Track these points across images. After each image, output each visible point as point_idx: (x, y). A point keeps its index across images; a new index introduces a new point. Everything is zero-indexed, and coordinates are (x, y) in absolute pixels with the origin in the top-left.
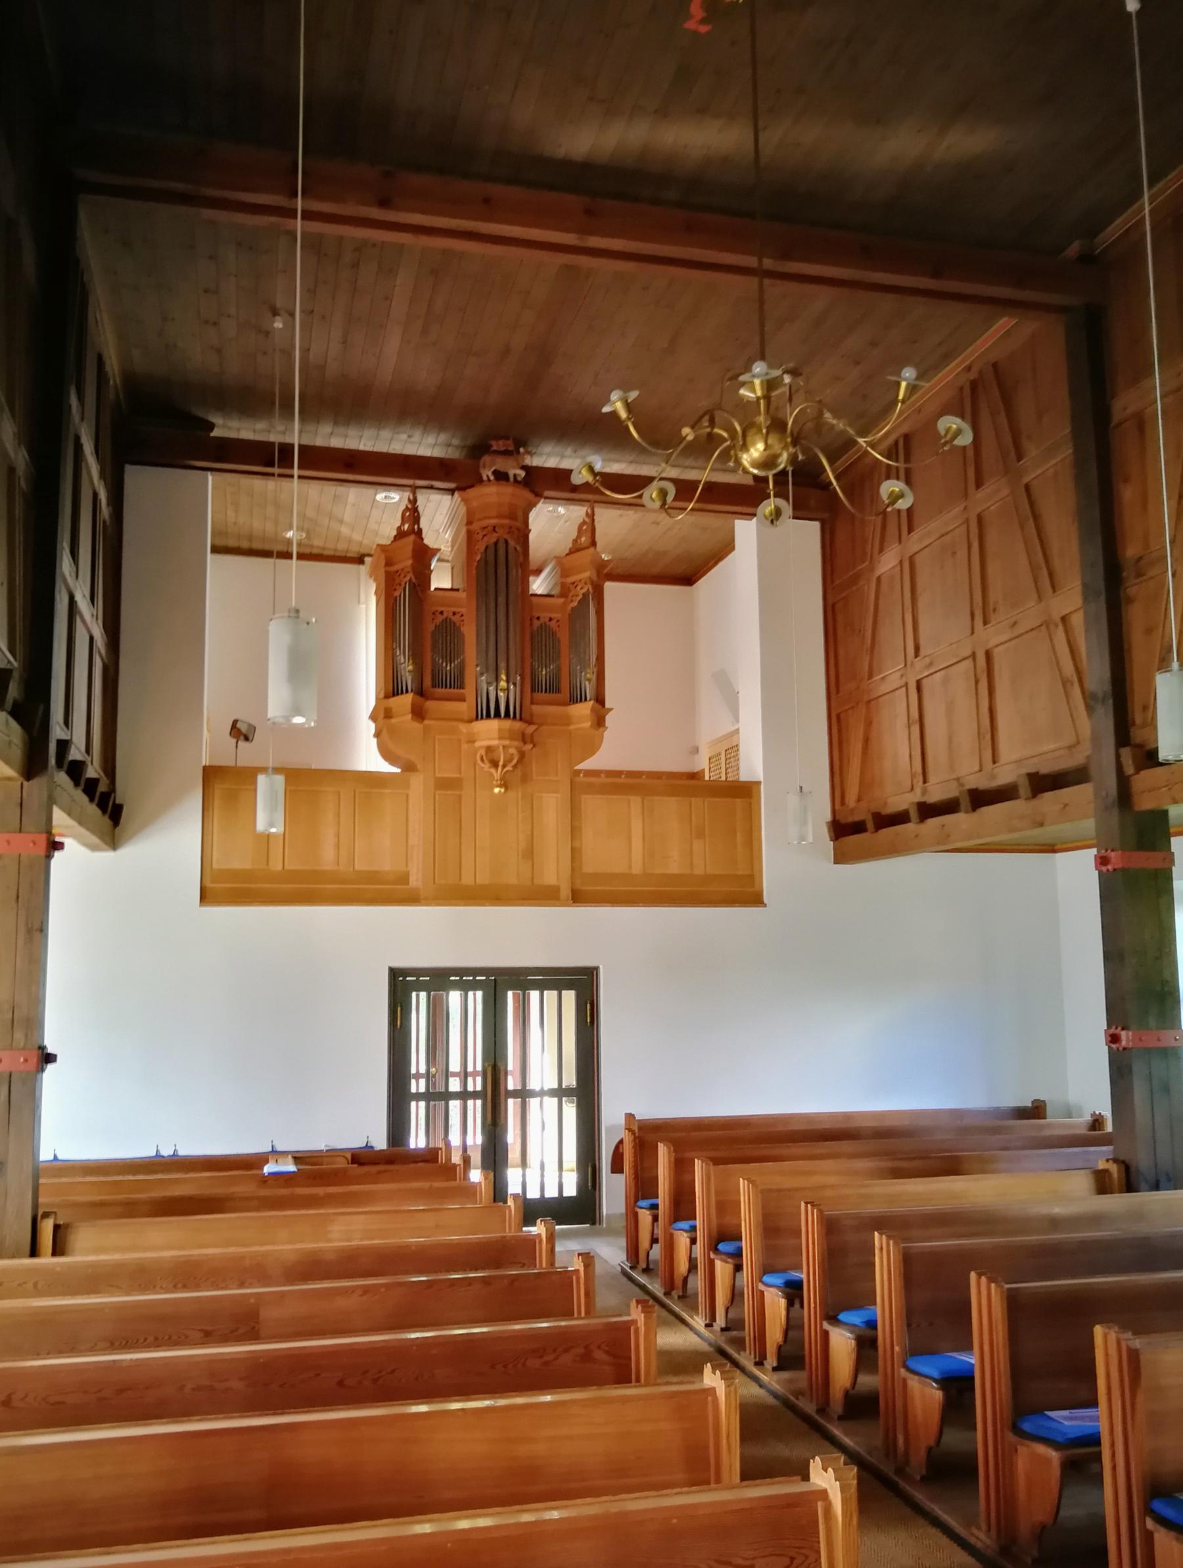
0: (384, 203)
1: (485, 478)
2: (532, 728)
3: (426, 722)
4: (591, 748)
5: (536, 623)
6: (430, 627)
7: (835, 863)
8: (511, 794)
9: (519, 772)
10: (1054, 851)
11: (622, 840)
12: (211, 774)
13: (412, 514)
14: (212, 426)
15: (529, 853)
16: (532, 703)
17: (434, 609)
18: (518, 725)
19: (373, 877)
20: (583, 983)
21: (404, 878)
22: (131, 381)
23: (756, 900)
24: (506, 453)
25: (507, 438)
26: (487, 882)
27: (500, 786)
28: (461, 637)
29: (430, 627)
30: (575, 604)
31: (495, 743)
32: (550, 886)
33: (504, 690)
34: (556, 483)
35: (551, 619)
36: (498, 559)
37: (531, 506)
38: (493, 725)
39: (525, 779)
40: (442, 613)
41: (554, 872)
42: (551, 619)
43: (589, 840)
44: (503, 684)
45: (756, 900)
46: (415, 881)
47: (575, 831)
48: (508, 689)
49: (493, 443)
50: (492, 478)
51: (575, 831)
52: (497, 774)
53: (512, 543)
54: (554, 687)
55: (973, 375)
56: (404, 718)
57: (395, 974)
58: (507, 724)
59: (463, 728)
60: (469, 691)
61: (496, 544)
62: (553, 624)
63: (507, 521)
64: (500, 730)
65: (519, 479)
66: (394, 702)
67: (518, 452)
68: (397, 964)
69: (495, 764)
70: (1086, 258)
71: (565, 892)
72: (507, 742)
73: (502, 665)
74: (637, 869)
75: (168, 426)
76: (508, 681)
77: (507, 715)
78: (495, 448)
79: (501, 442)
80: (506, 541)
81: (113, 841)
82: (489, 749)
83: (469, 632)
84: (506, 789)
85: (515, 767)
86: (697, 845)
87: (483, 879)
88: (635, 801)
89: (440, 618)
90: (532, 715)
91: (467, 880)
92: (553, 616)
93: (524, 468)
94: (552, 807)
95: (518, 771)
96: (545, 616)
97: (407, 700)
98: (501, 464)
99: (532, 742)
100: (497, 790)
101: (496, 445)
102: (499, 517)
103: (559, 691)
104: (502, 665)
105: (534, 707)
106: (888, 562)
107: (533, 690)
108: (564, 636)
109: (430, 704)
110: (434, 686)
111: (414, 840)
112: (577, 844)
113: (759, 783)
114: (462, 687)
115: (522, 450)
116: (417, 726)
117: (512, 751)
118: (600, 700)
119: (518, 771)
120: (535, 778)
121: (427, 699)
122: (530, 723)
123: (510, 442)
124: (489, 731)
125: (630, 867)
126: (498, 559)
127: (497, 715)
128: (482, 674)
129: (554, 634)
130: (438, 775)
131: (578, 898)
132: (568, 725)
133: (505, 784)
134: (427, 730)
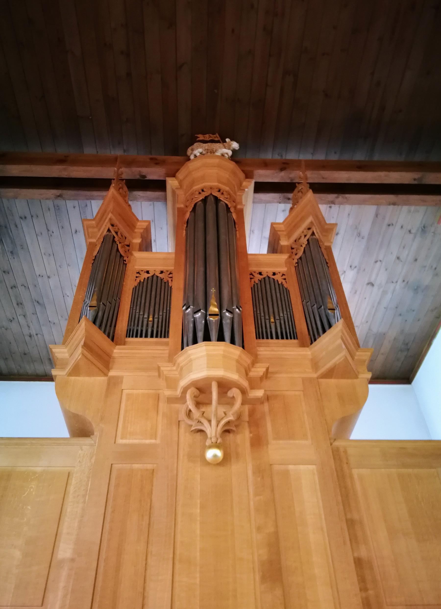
1: (192, 157)
3: (112, 373)
17: (138, 267)
18: (235, 351)
27: (217, 446)
29: (130, 284)
30: (300, 253)
39: (258, 442)
40: (148, 272)
42: (274, 274)
44: (214, 309)
48: (221, 315)
49: (199, 136)
52: (212, 431)
54: (288, 333)
61: (205, 201)
64: (209, 356)
72: (220, 373)
73: (213, 291)
76: (221, 309)
79: (207, 136)
89: (146, 276)
92: (276, 270)
101: (201, 137)
104: (213, 291)
109: (118, 351)
110: (130, 333)
112: (363, 553)
114: (166, 334)
115: (227, 140)
121: (117, 344)
123: (217, 135)
127: (207, 338)
129: (281, 286)
130: (120, 441)
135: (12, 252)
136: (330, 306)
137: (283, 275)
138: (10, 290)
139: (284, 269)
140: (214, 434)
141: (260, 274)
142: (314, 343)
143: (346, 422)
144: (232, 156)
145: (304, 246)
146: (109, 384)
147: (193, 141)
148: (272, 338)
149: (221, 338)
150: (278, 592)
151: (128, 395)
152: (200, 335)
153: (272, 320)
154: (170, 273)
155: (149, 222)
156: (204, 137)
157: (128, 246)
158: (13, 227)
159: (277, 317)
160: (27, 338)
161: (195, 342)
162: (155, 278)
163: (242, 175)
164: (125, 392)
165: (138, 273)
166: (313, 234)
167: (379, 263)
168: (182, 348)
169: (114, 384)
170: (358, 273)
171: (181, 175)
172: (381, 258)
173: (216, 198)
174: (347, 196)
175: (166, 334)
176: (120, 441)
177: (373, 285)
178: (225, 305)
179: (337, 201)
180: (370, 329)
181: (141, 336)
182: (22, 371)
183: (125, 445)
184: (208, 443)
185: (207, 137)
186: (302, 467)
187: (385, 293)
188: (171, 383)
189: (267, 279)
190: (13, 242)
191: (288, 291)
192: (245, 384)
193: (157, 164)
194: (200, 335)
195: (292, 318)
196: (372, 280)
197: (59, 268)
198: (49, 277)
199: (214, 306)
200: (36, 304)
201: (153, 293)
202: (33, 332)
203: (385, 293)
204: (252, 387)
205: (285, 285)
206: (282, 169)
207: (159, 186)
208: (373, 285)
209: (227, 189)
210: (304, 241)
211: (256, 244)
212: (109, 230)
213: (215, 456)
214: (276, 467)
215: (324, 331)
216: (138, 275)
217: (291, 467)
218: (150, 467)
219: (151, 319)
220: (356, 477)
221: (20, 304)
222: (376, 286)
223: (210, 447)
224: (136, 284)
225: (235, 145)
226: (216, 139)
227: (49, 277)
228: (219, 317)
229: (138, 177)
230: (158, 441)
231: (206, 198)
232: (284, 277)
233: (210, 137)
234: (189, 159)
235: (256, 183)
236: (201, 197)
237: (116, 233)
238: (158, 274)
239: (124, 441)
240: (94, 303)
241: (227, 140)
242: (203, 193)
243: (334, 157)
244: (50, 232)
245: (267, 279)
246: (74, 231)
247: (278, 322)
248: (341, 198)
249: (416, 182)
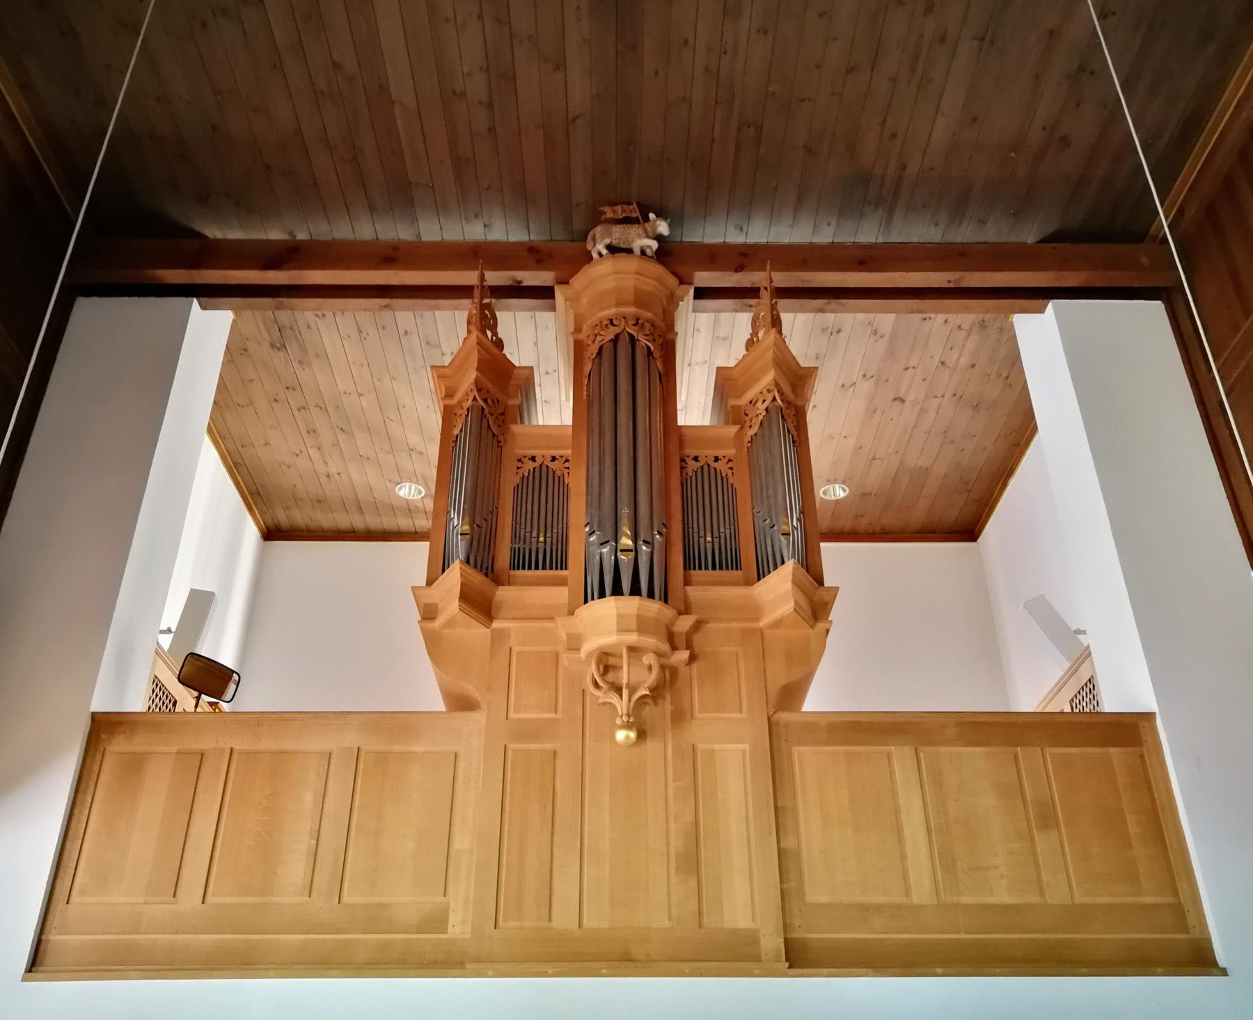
1: (595, 255)
2: (684, 624)
3: (496, 624)
5: (692, 466)
6: (510, 480)
8: (652, 746)
12: (103, 727)
15: (692, 860)
17: (520, 452)
18: (654, 607)
19: (375, 918)
21: (437, 921)
24: (627, 221)
25: (630, 204)
26: (605, 924)
27: (628, 726)
29: (510, 480)
30: (755, 430)
32: (736, 932)
35: (717, 459)
38: (608, 608)
39: (680, 717)
40: (533, 459)
41: (744, 903)
42: (717, 459)
44: (626, 542)
45: (1198, 959)
47: (782, 816)
49: (606, 209)
50: (604, 252)
51: (782, 816)
52: (622, 705)
53: (643, 340)
54: (727, 560)
56: (452, 607)
58: (631, 605)
62: (721, 466)
63: (631, 310)
64: (620, 617)
65: (649, 252)
67: (647, 219)
71: (772, 943)
72: (633, 638)
73: (625, 512)
74: (922, 893)
76: (635, 538)
78: (609, 215)
79: (618, 208)
80: (633, 340)
83: (577, 483)
84: (642, 735)
86: (1044, 842)
89: (531, 465)
91: (565, 919)
92: (720, 453)
93: (659, 238)
96: (707, 453)
98: (618, 234)
99: (689, 646)
100: (621, 735)
102: (619, 304)
103: (737, 566)
104: (625, 512)
105: (688, 588)
107: (687, 567)
108: (740, 481)
109: (504, 594)
110: (515, 566)
111: (462, 841)
112: (789, 843)
113: (1149, 717)
114: (563, 565)
115: (652, 216)
116: (475, 632)
120: (697, 715)
124: (607, 621)
125: (907, 893)
127: (617, 591)
128: (592, 533)
131: (798, 957)
132: (757, 619)
135: (300, 362)
136: (784, 528)
137: (730, 460)
138: (296, 413)
139: (731, 452)
140: (625, 712)
141: (696, 459)
142: (763, 580)
143: (792, 694)
144: (657, 252)
145: (761, 417)
146: (492, 640)
147: (596, 219)
148: (706, 568)
149: (635, 591)
150: (694, 883)
151: (518, 653)
152: (608, 589)
153: (709, 539)
154: (567, 461)
155: (532, 368)
156: (614, 211)
157: (503, 414)
158: (303, 329)
159: (716, 534)
160: (324, 479)
161: (602, 595)
162: (544, 469)
163: (672, 281)
164: (515, 649)
165: (519, 460)
166: (774, 399)
167: (911, 371)
168: (586, 602)
169: (499, 638)
170: (876, 384)
171: (578, 281)
172: (913, 363)
173: (632, 337)
174: (843, 301)
175: (563, 565)
176: (512, 715)
177: (903, 401)
178: (642, 536)
179: (828, 307)
180: (902, 463)
181: (530, 568)
182: (312, 525)
183: (519, 720)
184: (618, 721)
185: (619, 211)
186: (731, 746)
187: (923, 411)
188: (574, 644)
189: (706, 468)
190: (303, 349)
191: (734, 491)
192: (665, 647)
193: (539, 261)
194: (608, 589)
195: (735, 535)
196: (901, 395)
197: (377, 383)
198: (360, 395)
199: (627, 536)
200: (338, 431)
201: (543, 495)
202: (333, 469)
203: (923, 411)
204: (674, 648)
205: (731, 481)
206: (739, 268)
207: (545, 293)
208: (903, 401)
209: (649, 315)
210: (761, 407)
211: (694, 406)
212: (475, 399)
213: (627, 737)
214: (701, 747)
215: (776, 567)
216: (519, 465)
217: (717, 747)
218: (549, 746)
219: (542, 539)
220: (795, 756)
221: (312, 432)
222: (907, 406)
223: (621, 727)
224: (518, 480)
225: (663, 228)
226: (634, 215)
227: (360, 395)
228: (632, 555)
229: (509, 283)
230: (559, 716)
231: (617, 336)
232: (730, 465)
233: (624, 211)
234: (589, 258)
235: (696, 289)
236: (610, 334)
237: (485, 400)
238: (548, 462)
239: (518, 716)
240: (467, 528)
241: (652, 216)
242: (612, 328)
243: (825, 236)
244: (364, 334)
245: (706, 468)
246: (402, 332)
247: (716, 541)
248: (834, 303)
249: (951, 285)
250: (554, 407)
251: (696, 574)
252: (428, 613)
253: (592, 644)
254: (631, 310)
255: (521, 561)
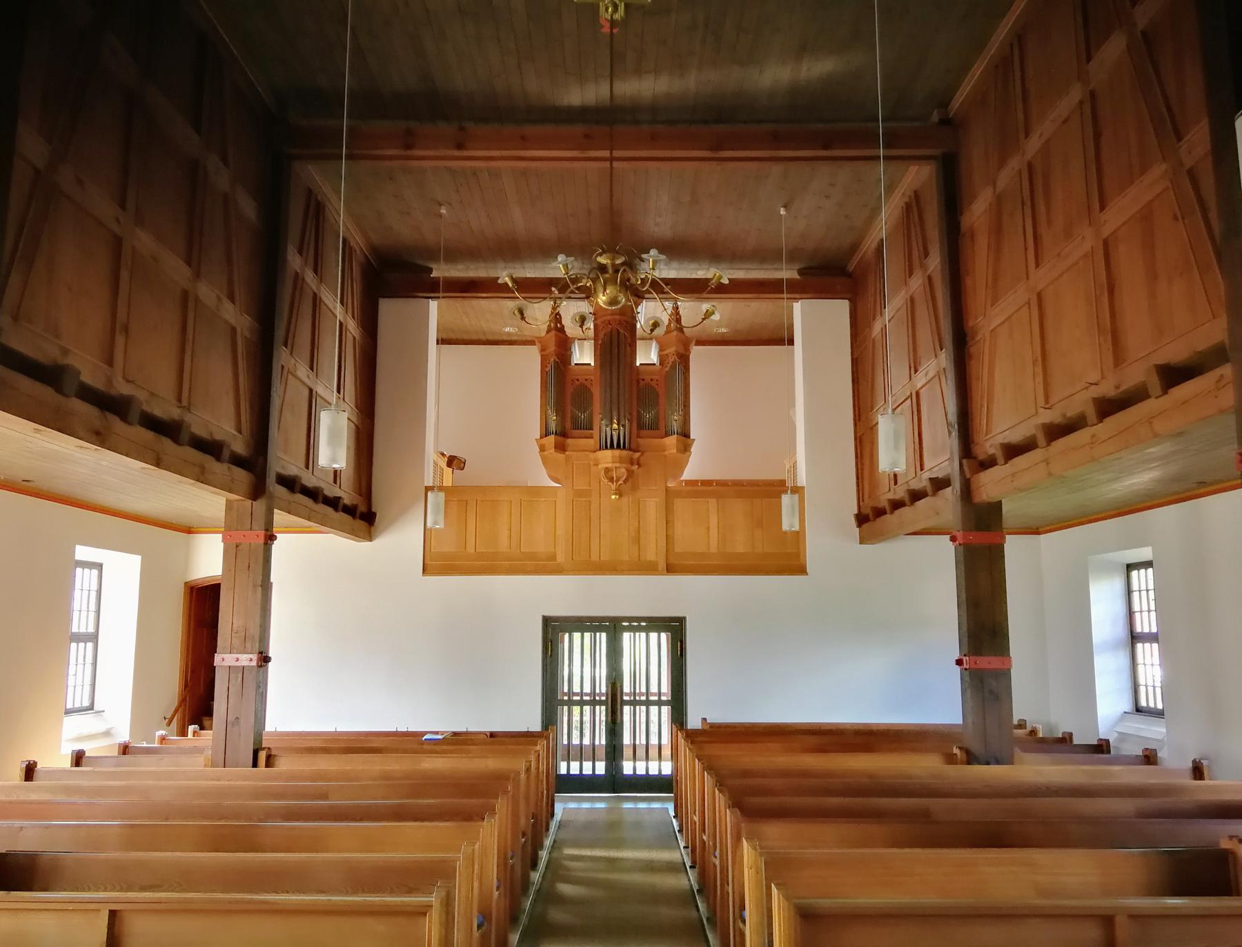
0: (460, 147)
4: (681, 466)
7: (861, 543)
8: (625, 499)
9: (629, 484)
10: (1038, 533)
11: (700, 528)
13: (557, 318)
14: (431, 270)
15: (637, 540)
16: (638, 436)
18: (625, 453)
19: (533, 556)
20: (675, 628)
22: (374, 249)
23: (802, 570)
28: (591, 394)
29: (570, 390)
31: (609, 465)
33: (614, 429)
34: (659, 287)
36: (617, 339)
37: (637, 305)
39: (635, 488)
41: (653, 550)
43: (679, 530)
44: (615, 426)
45: (802, 570)
46: (561, 558)
52: (614, 487)
54: (654, 426)
55: (907, 200)
56: (551, 451)
57: (547, 621)
58: (617, 452)
59: (592, 456)
60: (595, 432)
62: (653, 383)
63: (617, 317)
66: (545, 440)
68: (546, 614)
69: (611, 480)
70: (946, 122)
74: (714, 549)
75: (393, 275)
77: (619, 446)
81: (370, 537)
82: (607, 470)
83: (597, 392)
84: (621, 496)
85: (625, 481)
87: (605, 557)
88: (712, 503)
90: (638, 445)
91: (595, 557)
94: (652, 506)
95: (629, 483)
96: (648, 378)
97: (552, 438)
106: (877, 328)
109: (569, 441)
116: (561, 456)
117: (623, 470)
118: (685, 434)
119: (629, 483)
122: (635, 451)
126: (617, 339)
127: (612, 447)
131: (670, 569)
133: (620, 493)
134: (567, 459)
149: (619, 446)
250: (584, 355)
251: (643, 432)
252: (542, 449)
253: (602, 466)
254: (617, 317)
255: (577, 426)
